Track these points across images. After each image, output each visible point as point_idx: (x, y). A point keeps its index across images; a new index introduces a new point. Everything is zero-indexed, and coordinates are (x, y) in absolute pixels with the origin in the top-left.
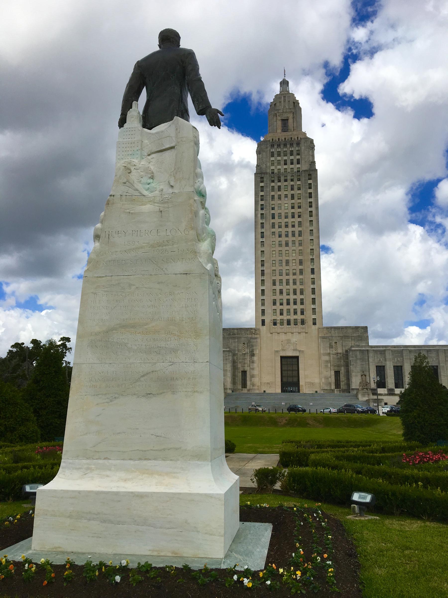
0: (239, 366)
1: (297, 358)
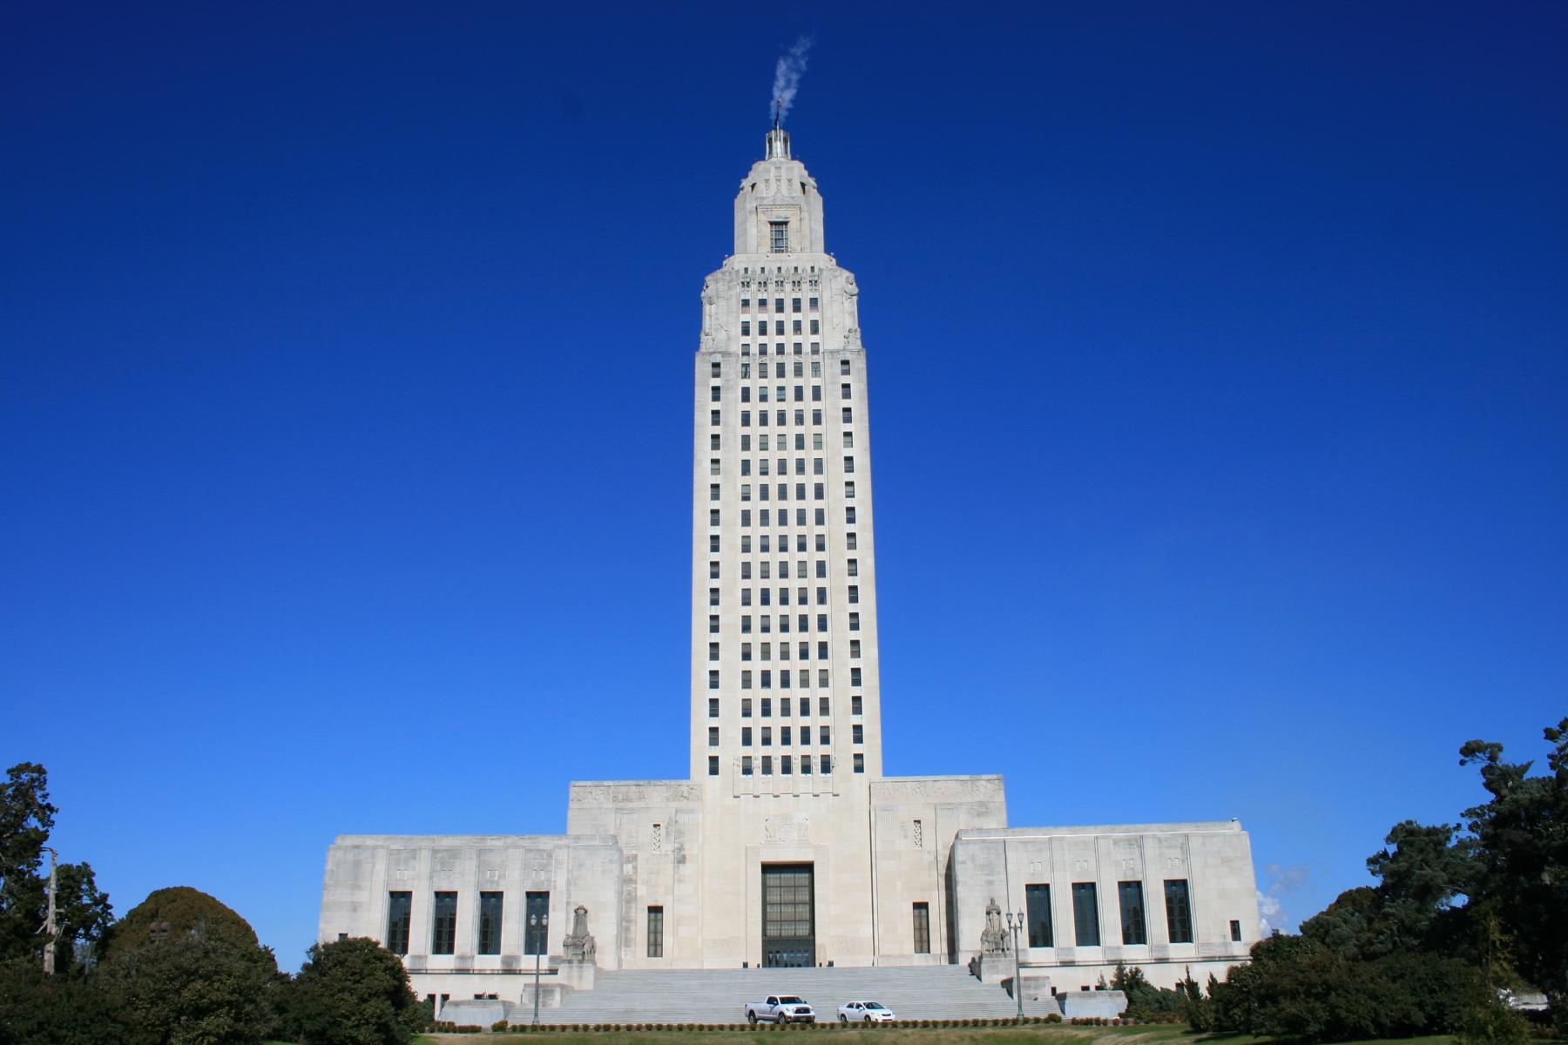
0: (642, 890)
1: (808, 868)
